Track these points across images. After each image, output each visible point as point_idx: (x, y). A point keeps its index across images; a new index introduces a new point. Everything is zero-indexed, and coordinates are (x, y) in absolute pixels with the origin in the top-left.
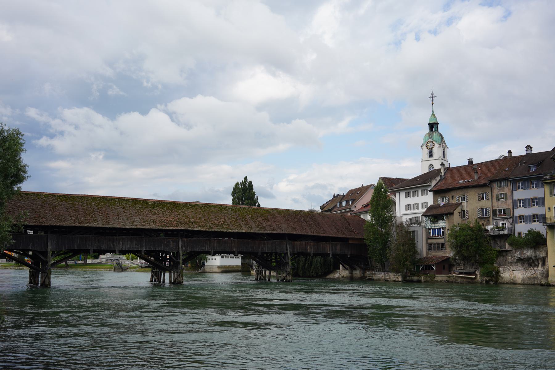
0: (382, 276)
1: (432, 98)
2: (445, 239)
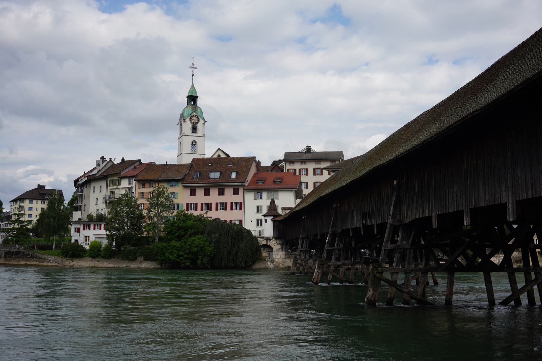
1: (192, 69)
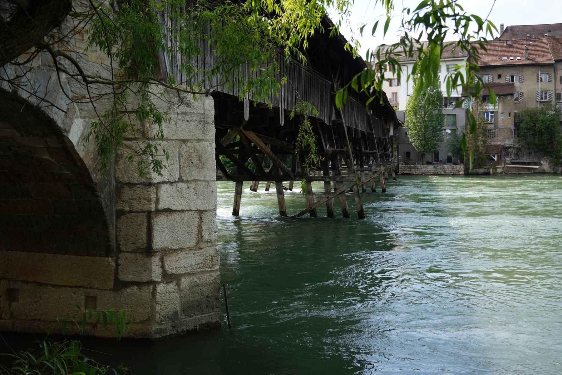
0: (429, 169)
2: (495, 125)
